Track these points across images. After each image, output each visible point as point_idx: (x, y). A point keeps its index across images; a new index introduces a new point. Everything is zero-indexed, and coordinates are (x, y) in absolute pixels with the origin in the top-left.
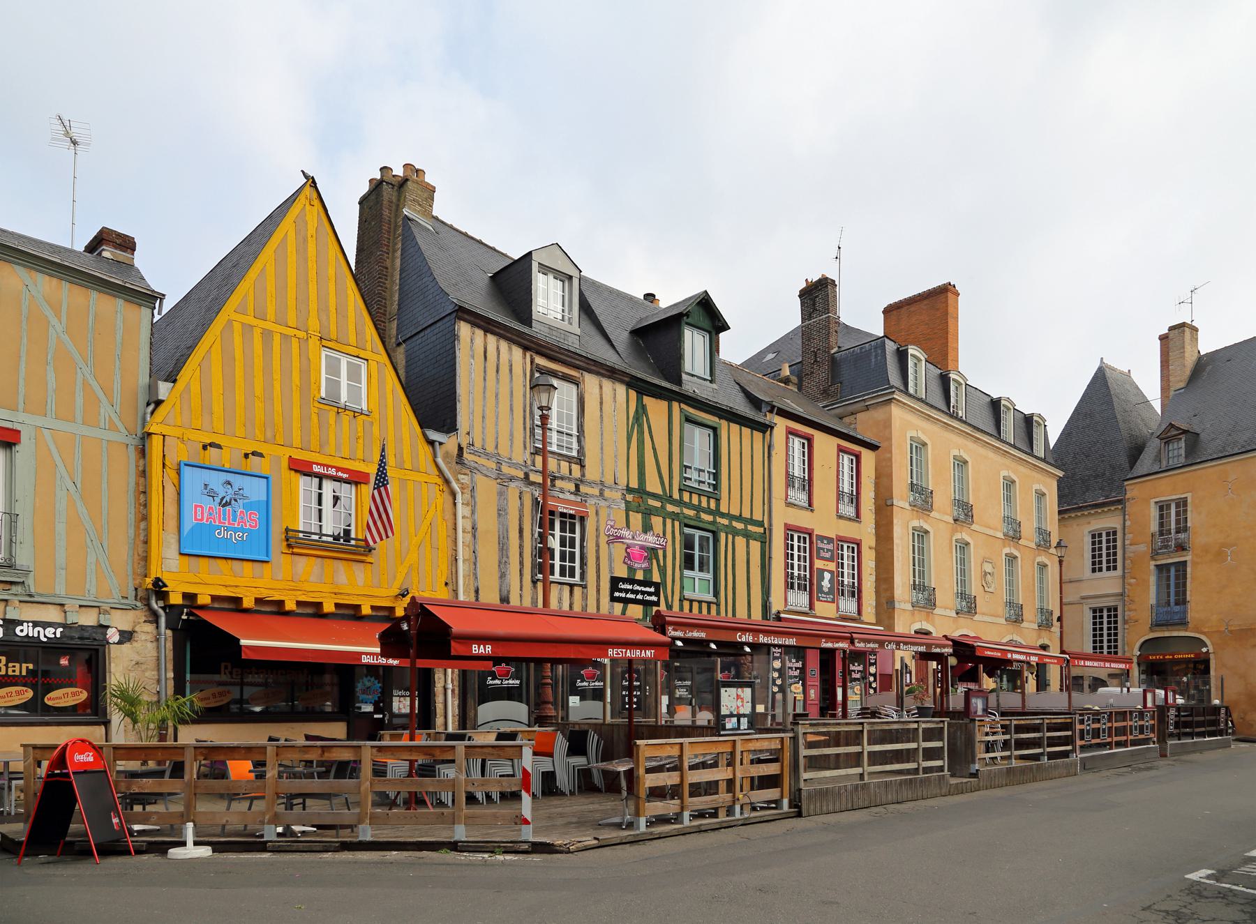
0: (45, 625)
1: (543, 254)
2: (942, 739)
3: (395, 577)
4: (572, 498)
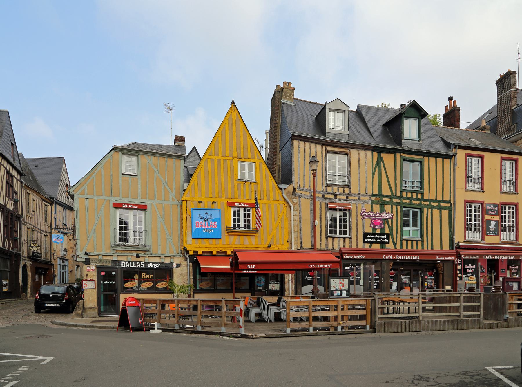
0: (155, 263)
1: (332, 104)
2: (479, 302)
3: (267, 240)
4: (345, 202)
